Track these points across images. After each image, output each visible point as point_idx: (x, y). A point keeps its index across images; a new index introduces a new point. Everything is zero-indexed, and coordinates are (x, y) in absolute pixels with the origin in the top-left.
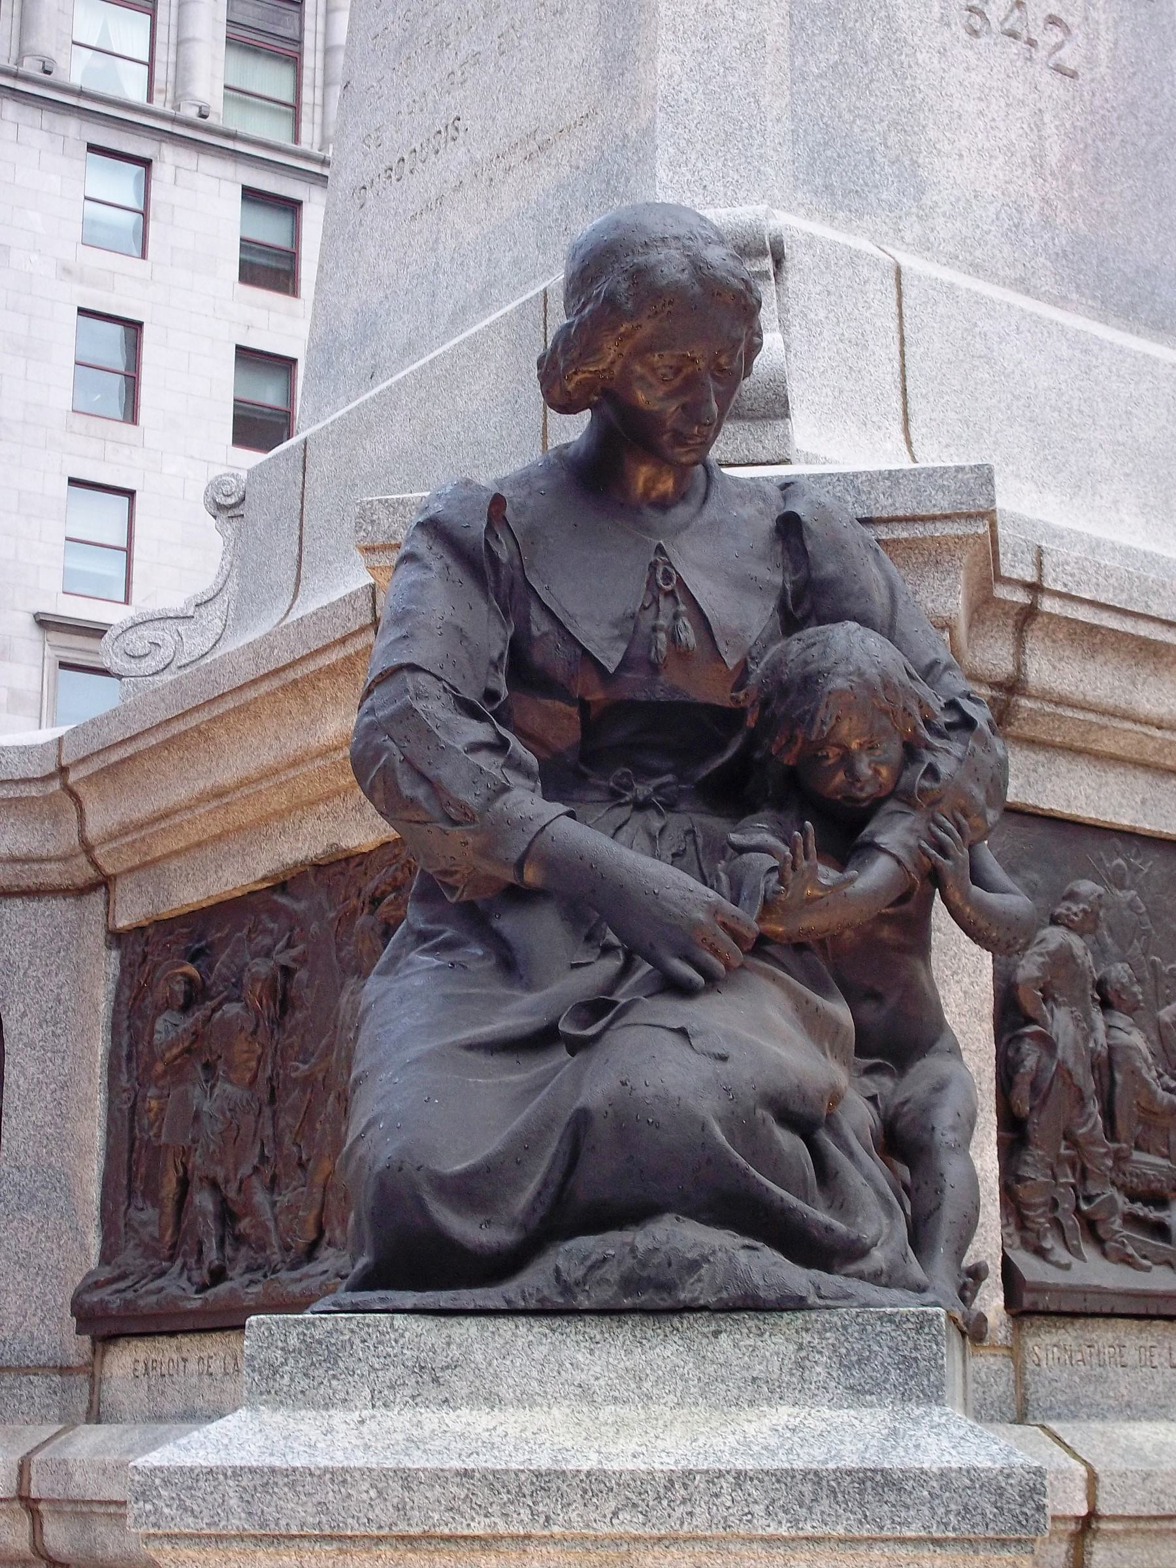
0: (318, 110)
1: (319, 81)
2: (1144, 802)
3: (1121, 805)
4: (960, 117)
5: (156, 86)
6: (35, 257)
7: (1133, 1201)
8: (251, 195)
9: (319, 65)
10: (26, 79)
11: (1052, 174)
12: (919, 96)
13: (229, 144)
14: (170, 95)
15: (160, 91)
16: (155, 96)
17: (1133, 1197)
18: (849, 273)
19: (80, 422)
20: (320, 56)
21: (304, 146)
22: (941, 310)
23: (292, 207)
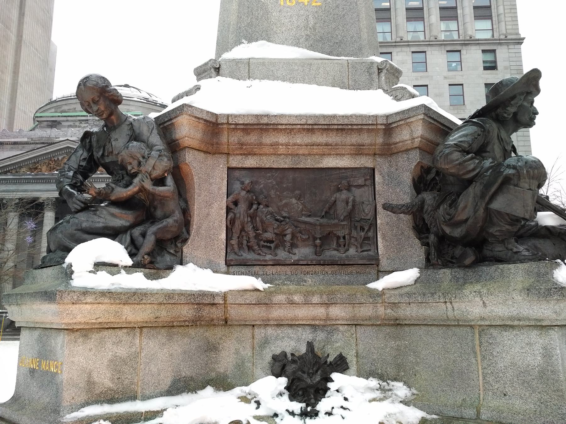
0: (497, 29)
1: (497, 23)
2: (273, 161)
3: (266, 163)
4: (283, 24)
5: (460, 34)
6: (438, 77)
7: (264, 242)
8: (484, 51)
9: (497, 19)
10: (432, 41)
11: (310, 28)
12: (272, 23)
13: (477, 42)
14: (463, 36)
15: (461, 35)
16: (460, 37)
17: (264, 242)
18: (235, 67)
19: (452, 108)
20: (496, 17)
21: (495, 38)
22: (260, 68)
23: (494, 51)
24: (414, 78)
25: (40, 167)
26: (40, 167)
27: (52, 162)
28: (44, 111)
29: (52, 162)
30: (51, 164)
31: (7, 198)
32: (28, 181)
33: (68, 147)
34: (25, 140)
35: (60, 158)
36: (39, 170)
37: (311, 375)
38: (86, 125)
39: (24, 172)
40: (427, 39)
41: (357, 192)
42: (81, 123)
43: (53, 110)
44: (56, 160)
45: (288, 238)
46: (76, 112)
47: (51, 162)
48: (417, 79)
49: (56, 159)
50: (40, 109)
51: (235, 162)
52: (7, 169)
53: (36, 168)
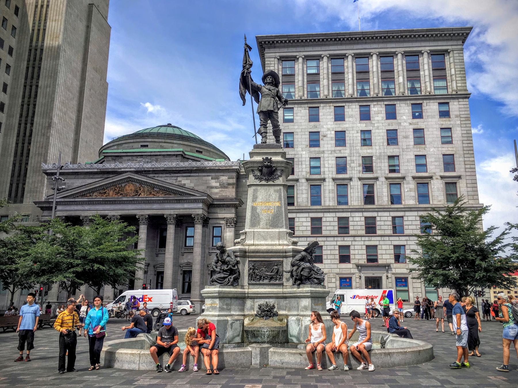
24: (387, 124)
25: (107, 192)
26: (107, 192)
31: (83, 215)
32: (99, 203)
34: (96, 170)
36: (107, 194)
37: (266, 308)
38: (141, 159)
40: (397, 95)
41: (279, 266)
42: (137, 158)
43: (116, 147)
45: (262, 278)
46: (134, 149)
47: (116, 188)
48: (389, 125)
51: (250, 259)
53: (105, 193)
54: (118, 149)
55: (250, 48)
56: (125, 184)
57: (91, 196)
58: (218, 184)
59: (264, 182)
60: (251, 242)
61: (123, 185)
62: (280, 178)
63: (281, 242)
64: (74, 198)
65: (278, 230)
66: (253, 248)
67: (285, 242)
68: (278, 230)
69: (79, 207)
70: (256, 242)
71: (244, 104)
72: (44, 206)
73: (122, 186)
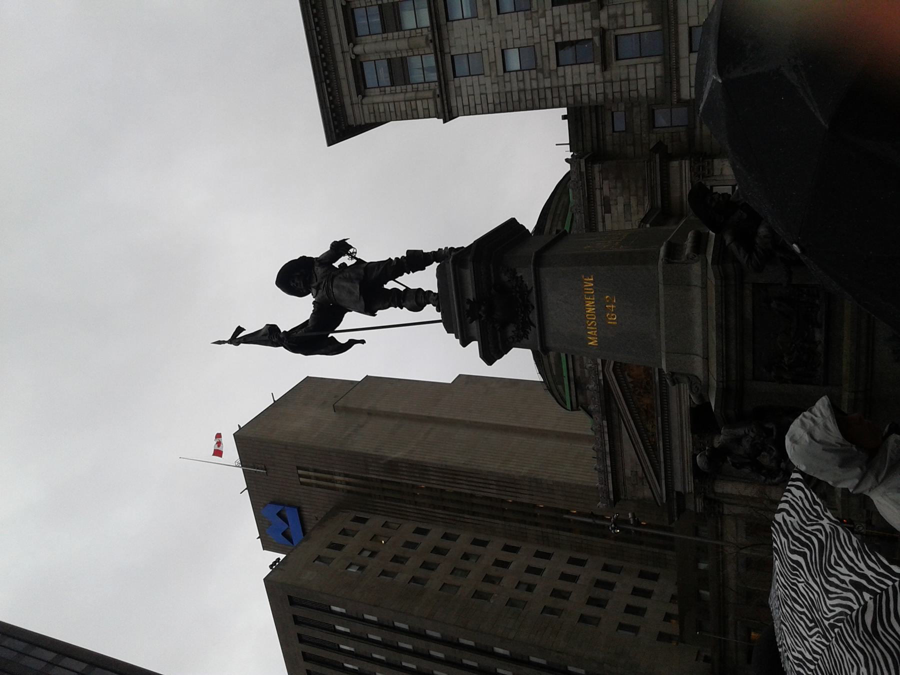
27: (637, 390)
28: (562, 398)
29: (637, 390)
30: (640, 392)
33: (613, 370)
35: (629, 380)
39: (653, 427)
43: (560, 387)
44: (632, 385)
49: (631, 385)
50: (560, 404)
52: (650, 447)
54: (563, 384)
55: (240, 330)
56: (628, 377)
57: (653, 435)
58: (621, 200)
59: (534, 316)
60: (698, 362)
61: (629, 380)
62: (519, 275)
63: (696, 281)
64: (659, 462)
65: (661, 286)
66: (713, 368)
67: (696, 268)
68: (661, 286)
69: (677, 454)
70: (698, 348)
71: (363, 342)
72: (675, 507)
73: (632, 382)
